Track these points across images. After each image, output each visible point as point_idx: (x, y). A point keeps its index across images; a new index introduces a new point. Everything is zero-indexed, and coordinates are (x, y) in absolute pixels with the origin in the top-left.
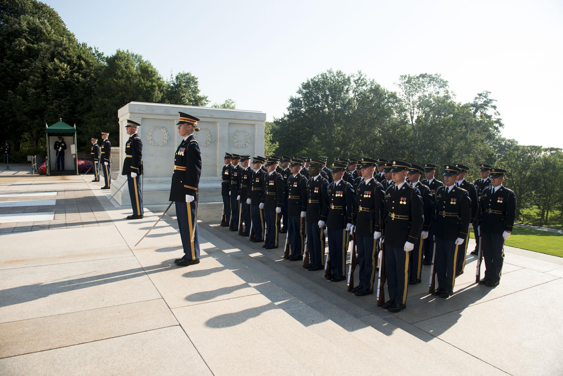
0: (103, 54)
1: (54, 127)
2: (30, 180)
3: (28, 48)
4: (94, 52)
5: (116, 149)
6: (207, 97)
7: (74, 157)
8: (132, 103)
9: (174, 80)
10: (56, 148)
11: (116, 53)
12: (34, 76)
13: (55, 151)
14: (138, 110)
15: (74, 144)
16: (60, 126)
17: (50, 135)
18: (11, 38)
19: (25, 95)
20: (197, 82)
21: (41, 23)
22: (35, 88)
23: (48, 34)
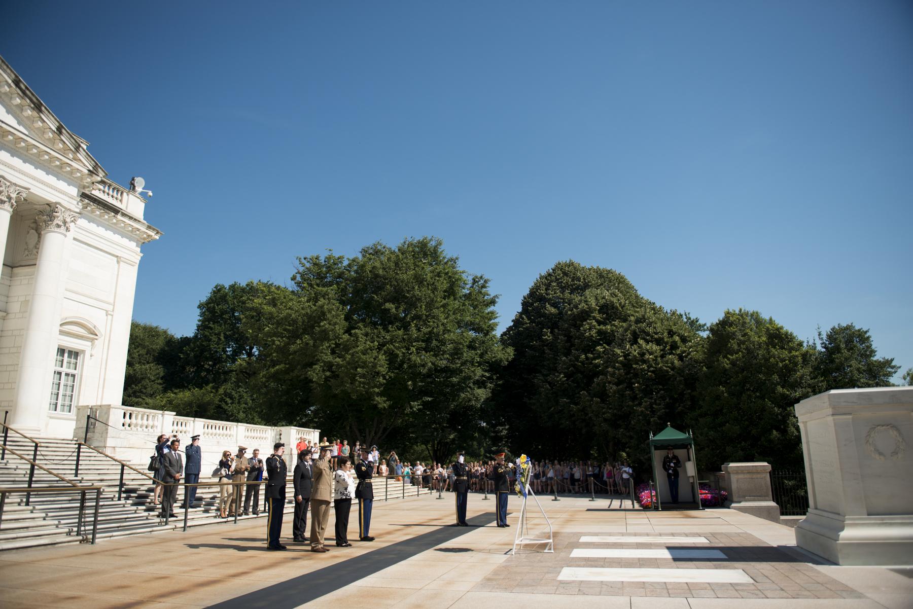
0: (697, 321)
1: (659, 437)
2: (641, 516)
3: (600, 332)
4: (685, 320)
5: (755, 466)
6: (892, 360)
7: (691, 480)
8: (833, 392)
9: (825, 341)
10: (666, 467)
11: (723, 315)
12: (614, 367)
13: (666, 473)
14: (845, 402)
15: (689, 460)
16: (670, 434)
17: (657, 448)
18: (578, 322)
19: (603, 395)
20: (868, 338)
21: (611, 294)
22: (617, 384)
23: (622, 308)
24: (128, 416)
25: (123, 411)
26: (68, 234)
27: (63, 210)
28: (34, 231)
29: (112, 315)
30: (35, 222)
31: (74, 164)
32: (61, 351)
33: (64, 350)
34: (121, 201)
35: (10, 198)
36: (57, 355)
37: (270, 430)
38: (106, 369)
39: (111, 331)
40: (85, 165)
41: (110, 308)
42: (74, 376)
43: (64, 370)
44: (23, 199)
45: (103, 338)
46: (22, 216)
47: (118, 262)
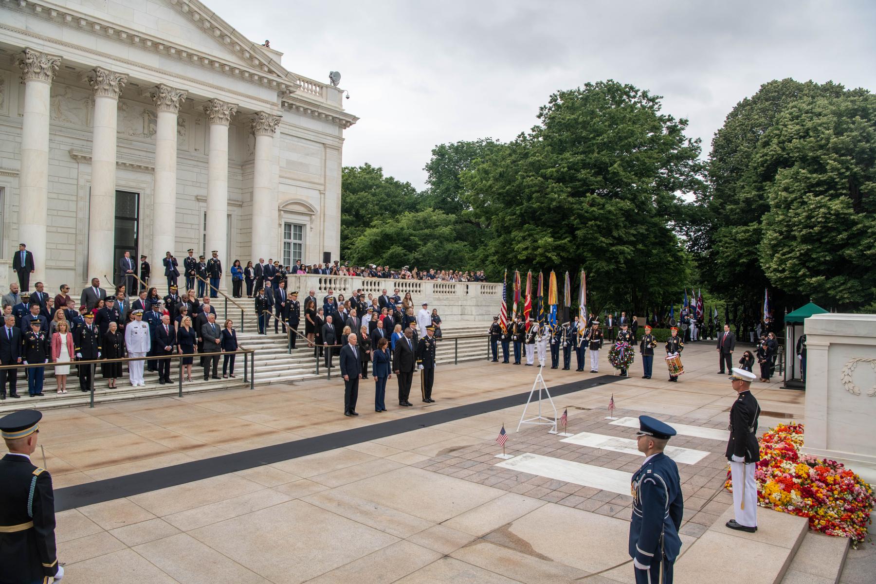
24: (323, 281)
25: (319, 278)
26: (274, 135)
27: (267, 115)
28: (252, 135)
29: (324, 194)
30: (252, 127)
31: (270, 77)
32: (288, 225)
33: (290, 226)
34: (321, 95)
35: (224, 114)
36: (285, 230)
37: (458, 285)
38: (324, 238)
39: (324, 206)
40: (278, 76)
41: (322, 188)
42: (301, 245)
43: (292, 241)
44: (234, 114)
45: (319, 213)
46: (244, 123)
47: (325, 148)
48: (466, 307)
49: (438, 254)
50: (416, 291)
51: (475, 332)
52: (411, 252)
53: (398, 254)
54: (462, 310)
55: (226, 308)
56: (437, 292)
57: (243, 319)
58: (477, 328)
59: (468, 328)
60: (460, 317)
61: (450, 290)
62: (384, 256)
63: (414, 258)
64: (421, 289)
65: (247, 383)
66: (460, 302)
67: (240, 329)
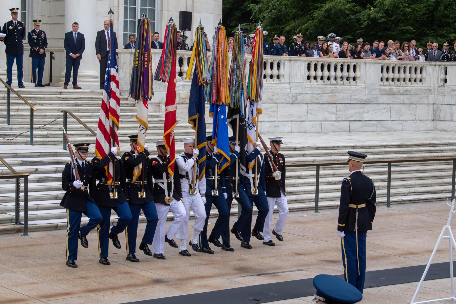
48: (442, 107)
49: (414, 10)
50: (348, 79)
51: (442, 151)
52: (364, 6)
53: (341, 11)
54: (435, 111)
55: (8, 104)
56: (387, 80)
57: (32, 123)
58: (448, 145)
59: (430, 145)
60: (430, 124)
61: (414, 76)
62: (316, 14)
63: (369, 18)
64: (358, 74)
65: (18, 226)
66: (431, 97)
67: (29, 139)
